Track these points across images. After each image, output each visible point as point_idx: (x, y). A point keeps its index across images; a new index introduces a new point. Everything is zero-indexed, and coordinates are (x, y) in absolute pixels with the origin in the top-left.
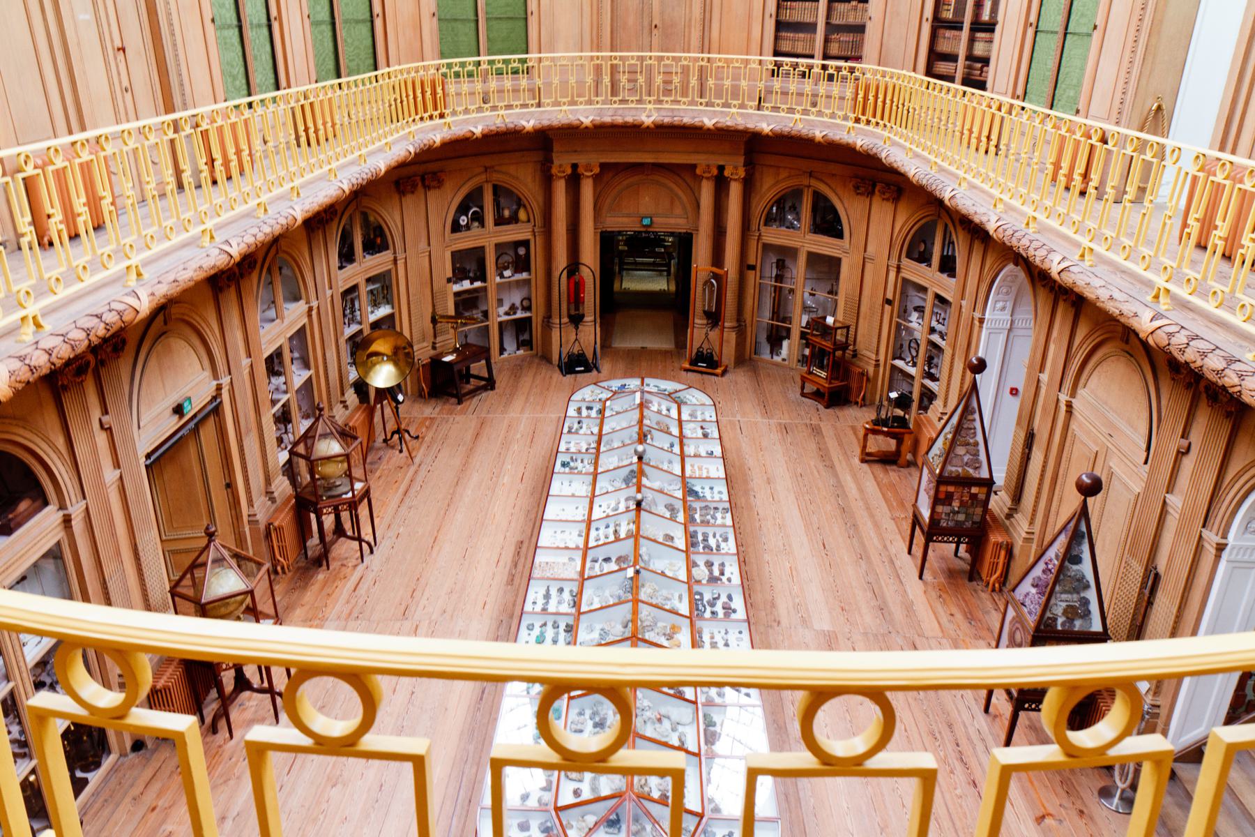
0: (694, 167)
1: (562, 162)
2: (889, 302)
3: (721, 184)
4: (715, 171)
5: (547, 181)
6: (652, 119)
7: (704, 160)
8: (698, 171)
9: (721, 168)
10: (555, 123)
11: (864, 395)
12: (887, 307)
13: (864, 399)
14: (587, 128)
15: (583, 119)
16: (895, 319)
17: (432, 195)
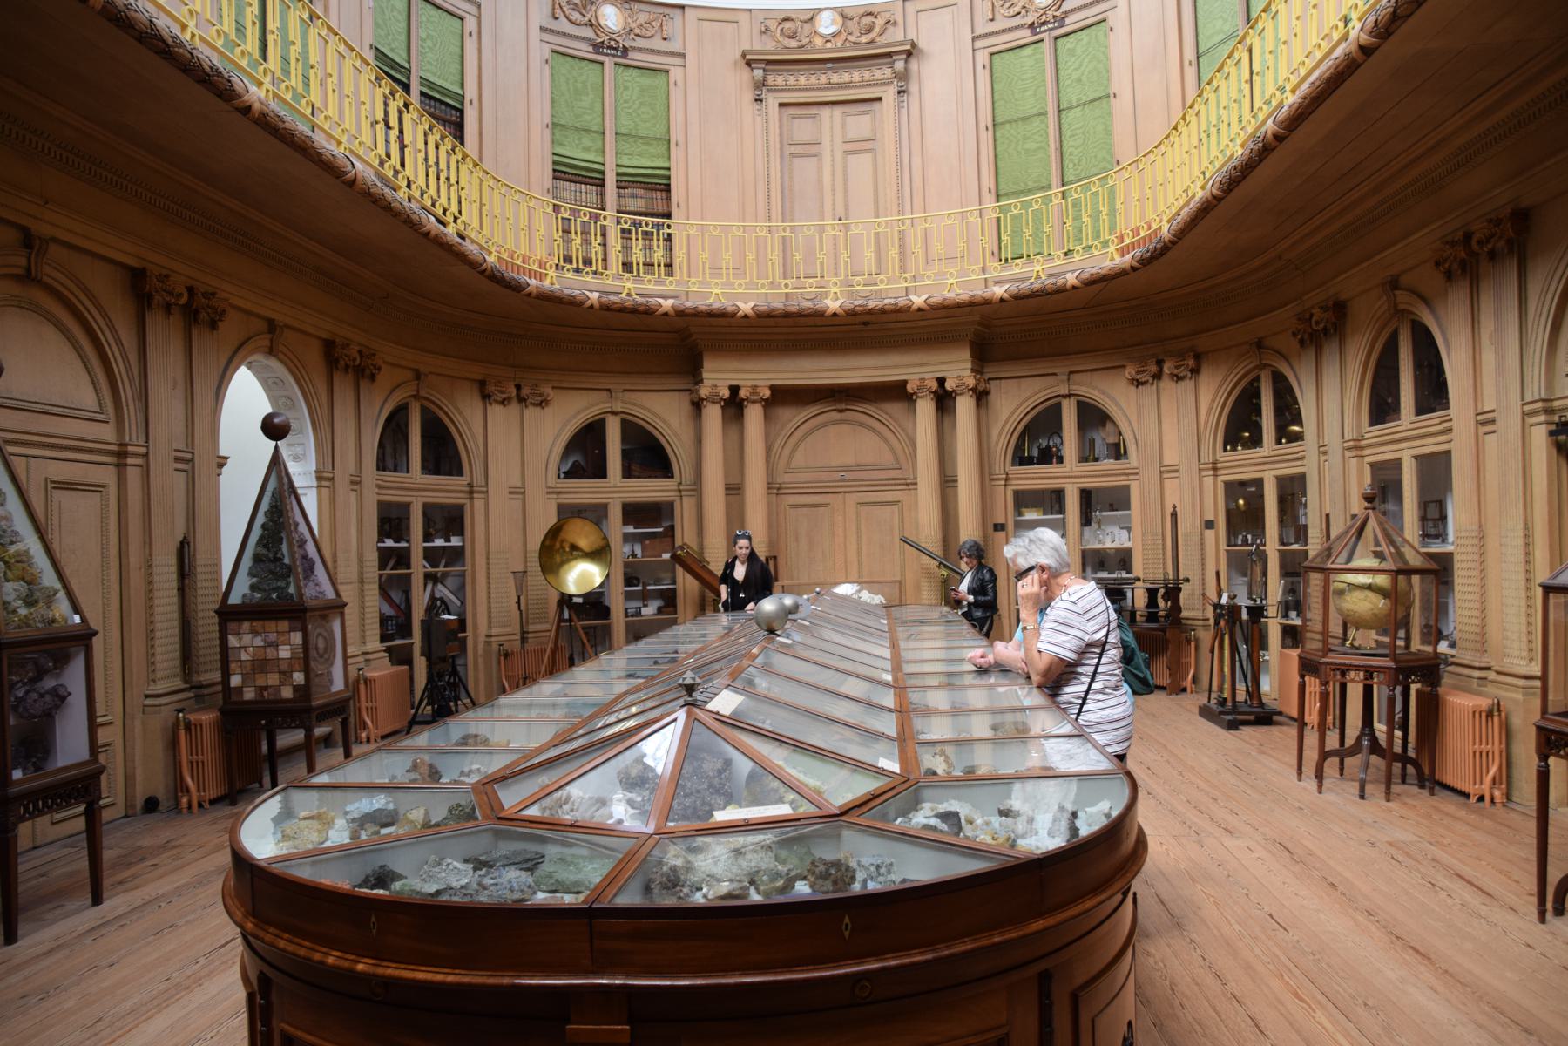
0: (903, 384)
1: (718, 376)
2: (1210, 525)
3: (944, 400)
4: (934, 385)
5: (697, 406)
6: (838, 303)
7: (916, 369)
8: (909, 388)
9: (941, 381)
10: (702, 304)
11: (1194, 677)
12: (1210, 534)
13: (1195, 680)
14: (746, 316)
15: (741, 305)
16: (1223, 546)
17: (531, 413)
